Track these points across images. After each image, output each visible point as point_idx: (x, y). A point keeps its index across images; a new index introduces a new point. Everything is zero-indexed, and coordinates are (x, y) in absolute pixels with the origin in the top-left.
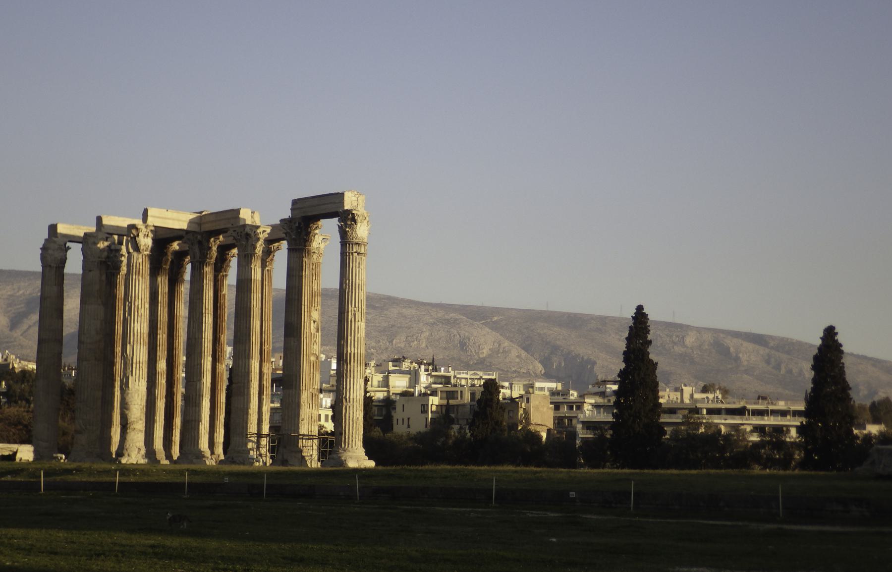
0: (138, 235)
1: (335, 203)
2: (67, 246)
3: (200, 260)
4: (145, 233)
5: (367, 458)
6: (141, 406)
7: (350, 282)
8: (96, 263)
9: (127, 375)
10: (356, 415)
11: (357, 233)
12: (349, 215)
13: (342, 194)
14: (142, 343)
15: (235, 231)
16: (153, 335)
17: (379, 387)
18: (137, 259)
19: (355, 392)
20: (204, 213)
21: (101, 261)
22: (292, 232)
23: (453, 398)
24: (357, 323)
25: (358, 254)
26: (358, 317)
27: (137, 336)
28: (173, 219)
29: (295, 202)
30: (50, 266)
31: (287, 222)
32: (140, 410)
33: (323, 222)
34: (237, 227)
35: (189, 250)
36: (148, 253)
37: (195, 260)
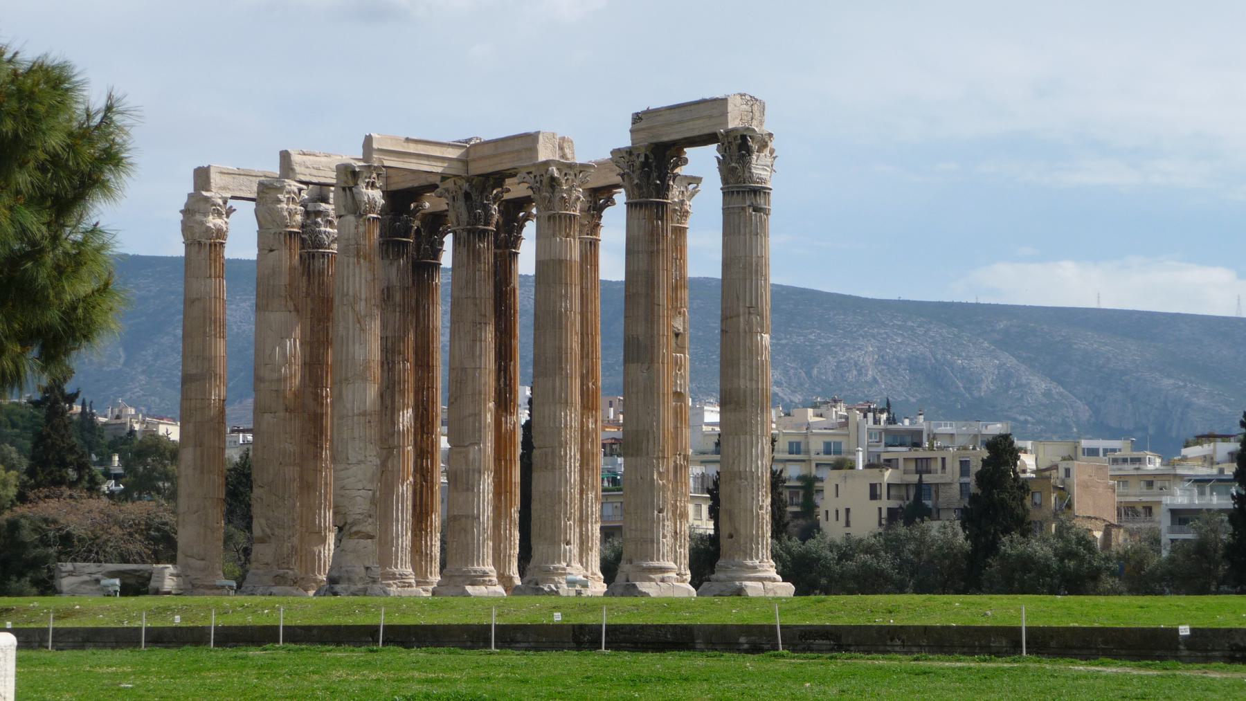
0: (356, 184)
1: (711, 117)
2: (228, 205)
3: (468, 227)
4: (367, 180)
5: (779, 578)
6: (370, 492)
8: (282, 237)
11: (753, 171)
16: (388, 363)
17: (791, 453)
20: (472, 143)
21: (291, 233)
22: (633, 171)
23: (929, 472)
29: (637, 118)
30: (199, 243)
31: (624, 155)
33: (690, 152)
34: (534, 165)
35: (447, 211)
36: (375, 216)
37: (461, 227)
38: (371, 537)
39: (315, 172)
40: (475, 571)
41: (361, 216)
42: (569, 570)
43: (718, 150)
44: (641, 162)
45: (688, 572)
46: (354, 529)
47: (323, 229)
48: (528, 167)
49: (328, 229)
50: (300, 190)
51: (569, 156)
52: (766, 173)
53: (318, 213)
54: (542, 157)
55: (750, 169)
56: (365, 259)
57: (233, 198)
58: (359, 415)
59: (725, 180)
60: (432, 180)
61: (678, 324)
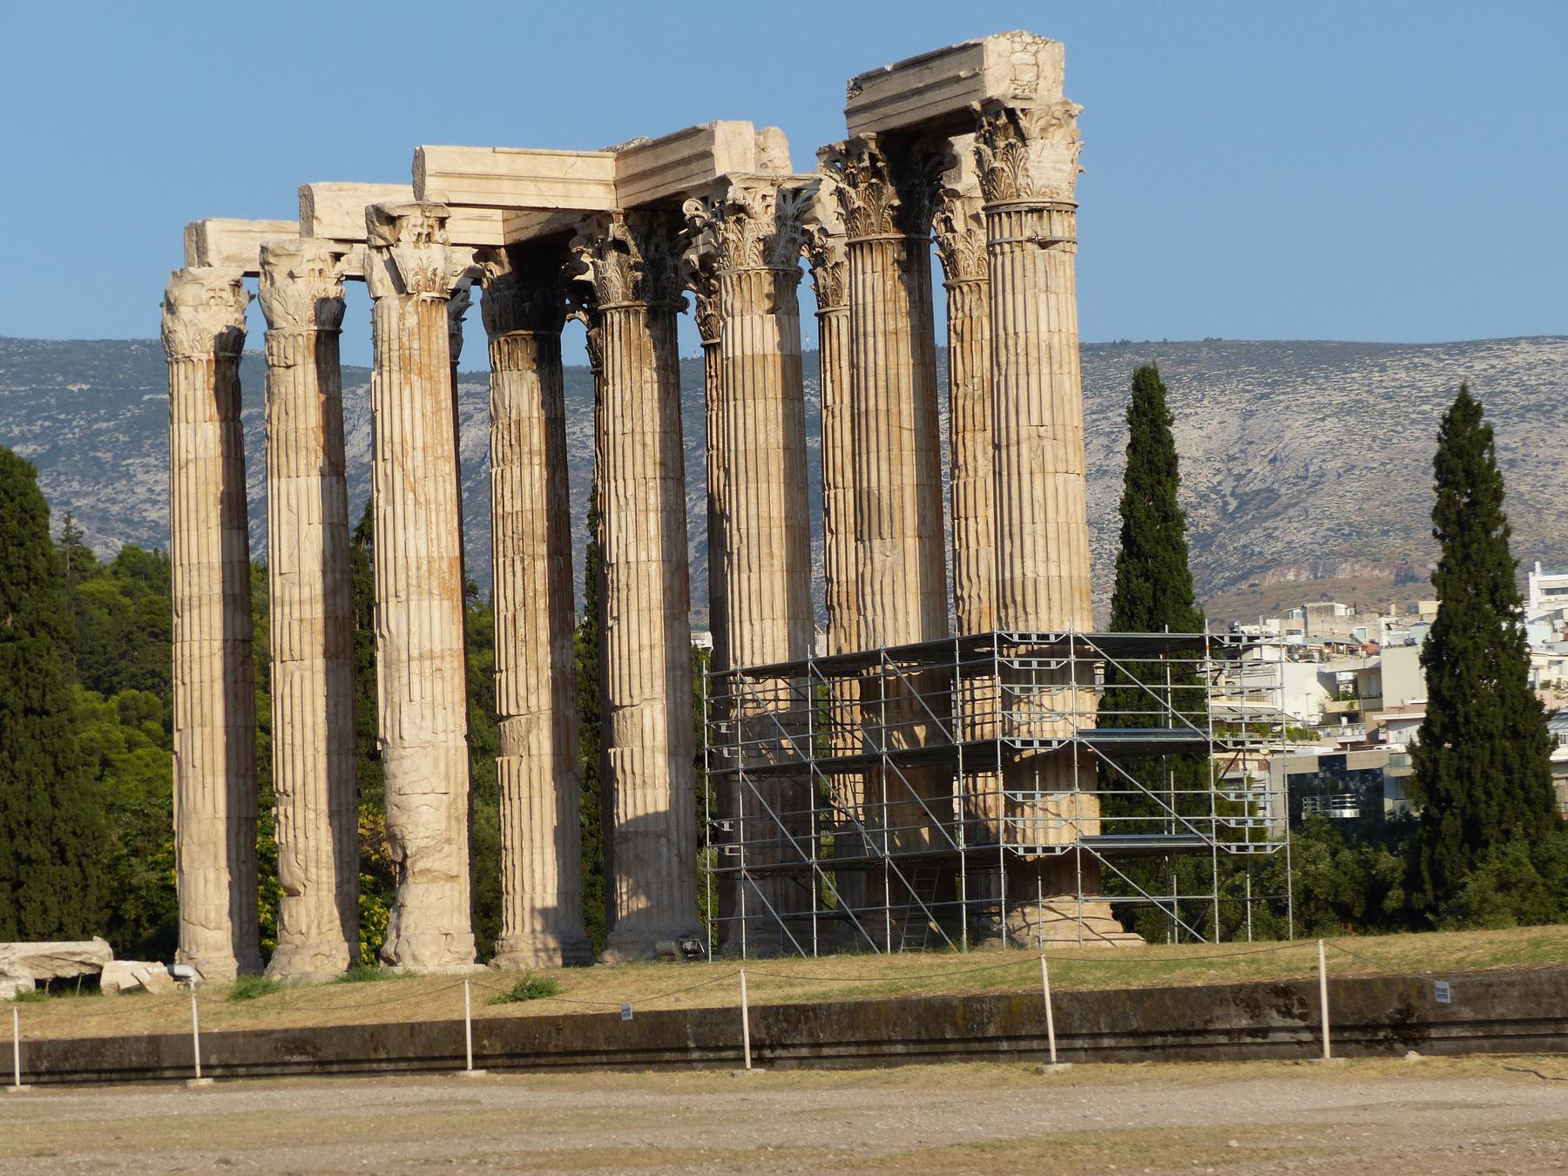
1: (958, 79)
4: (419, 230)
5: (1118, 926)
7: (1021, 342)
9: (396, 699)
12: (997, 117)
13: (972, 50)
14: (436, 591)
15: (704, 200)
16: (523, 560)
18: (402, 317)
22: (855, 186)
24: (1049, 477)
25: (1044, 245)
26: (1055, 457)
27: (418, 568)
28: (518, 178)
29: (858, 85)
32: (443, 809)
34: (706, 184)
36: (437, 295)
38: (453, 878)
44: (864, 169)
46: (420, 865)
48: (699, 187)
54: (719, 173)
55: (1026, 170)
56: (420, 374)
57: (247, 274)
58: (421, 657)
60: (566, 220)
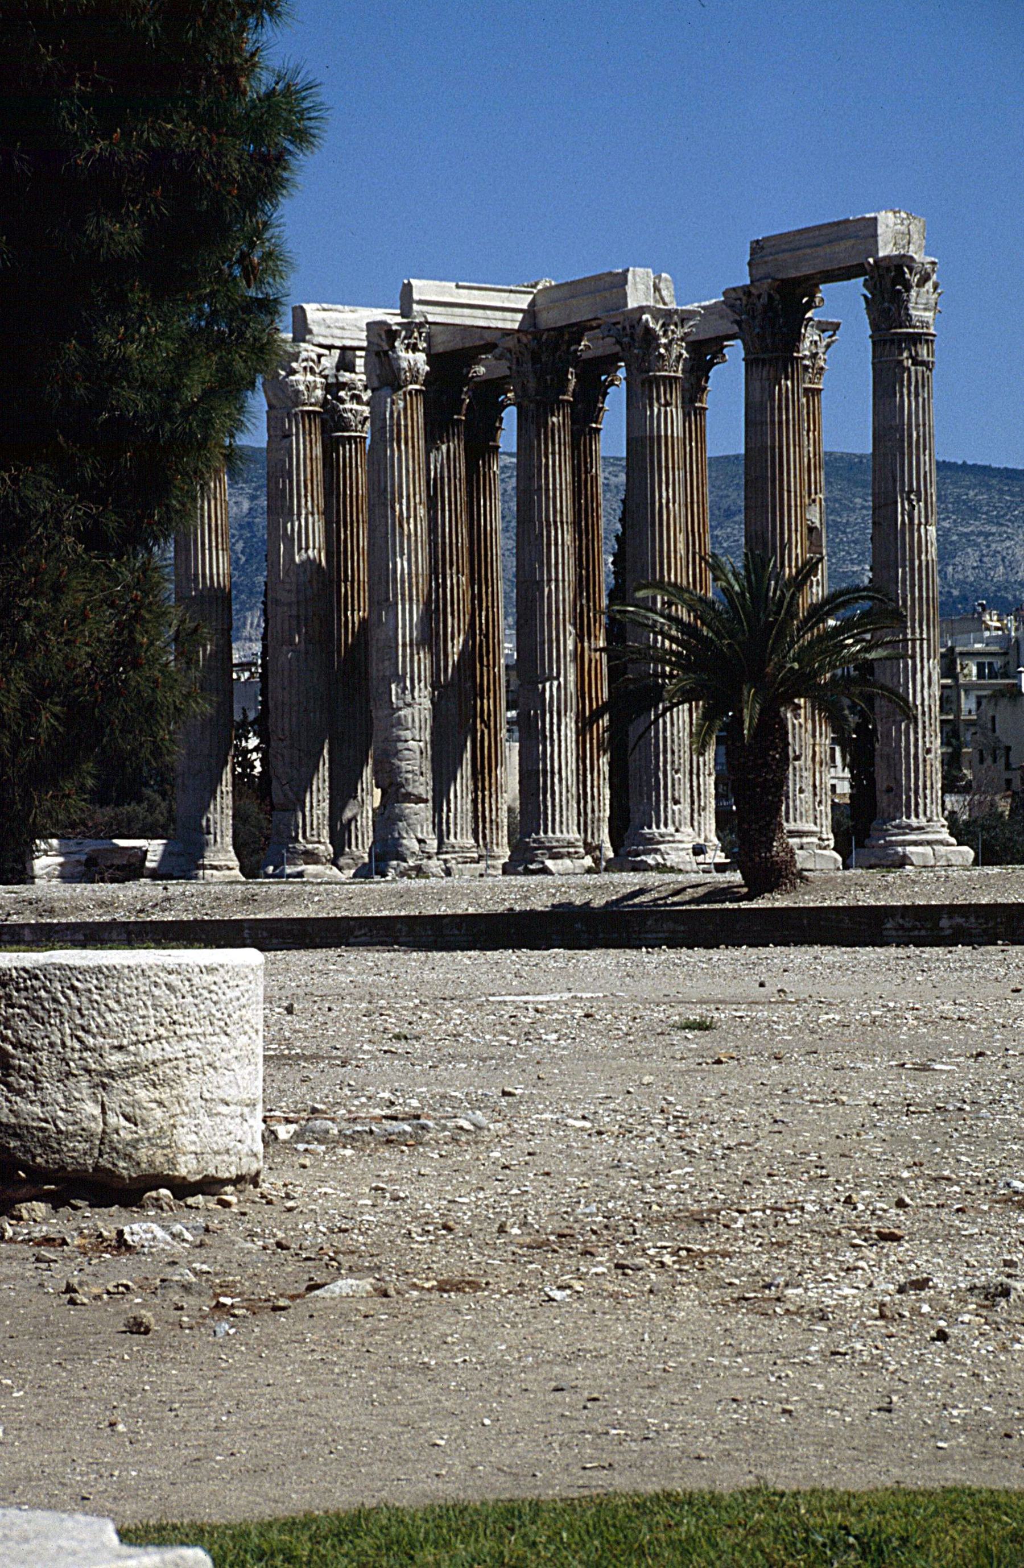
5: (953, 840)
6: (422, 744)
10: (924, 743)
11: (912, 312)
19: (919, 688)
31: (741, 294)
32: (418, 752)
33: (825, 290)
36: (417, 387)
38: (426, 801)
39: (338, 332)
40: (558, 841)
41: (400, 388)
42: (678, 836)
43: (865, 285)
45: (831, 836)
47: (348, 406)
49: (355, 406)
50: (320, 356)
51: (667, 300)
52: (927, 314)
53: (343, 386)
54: (632, 304)
55: (907, 309)
59: (874, 325)
60: (489, 337)
61: (814, 516)
